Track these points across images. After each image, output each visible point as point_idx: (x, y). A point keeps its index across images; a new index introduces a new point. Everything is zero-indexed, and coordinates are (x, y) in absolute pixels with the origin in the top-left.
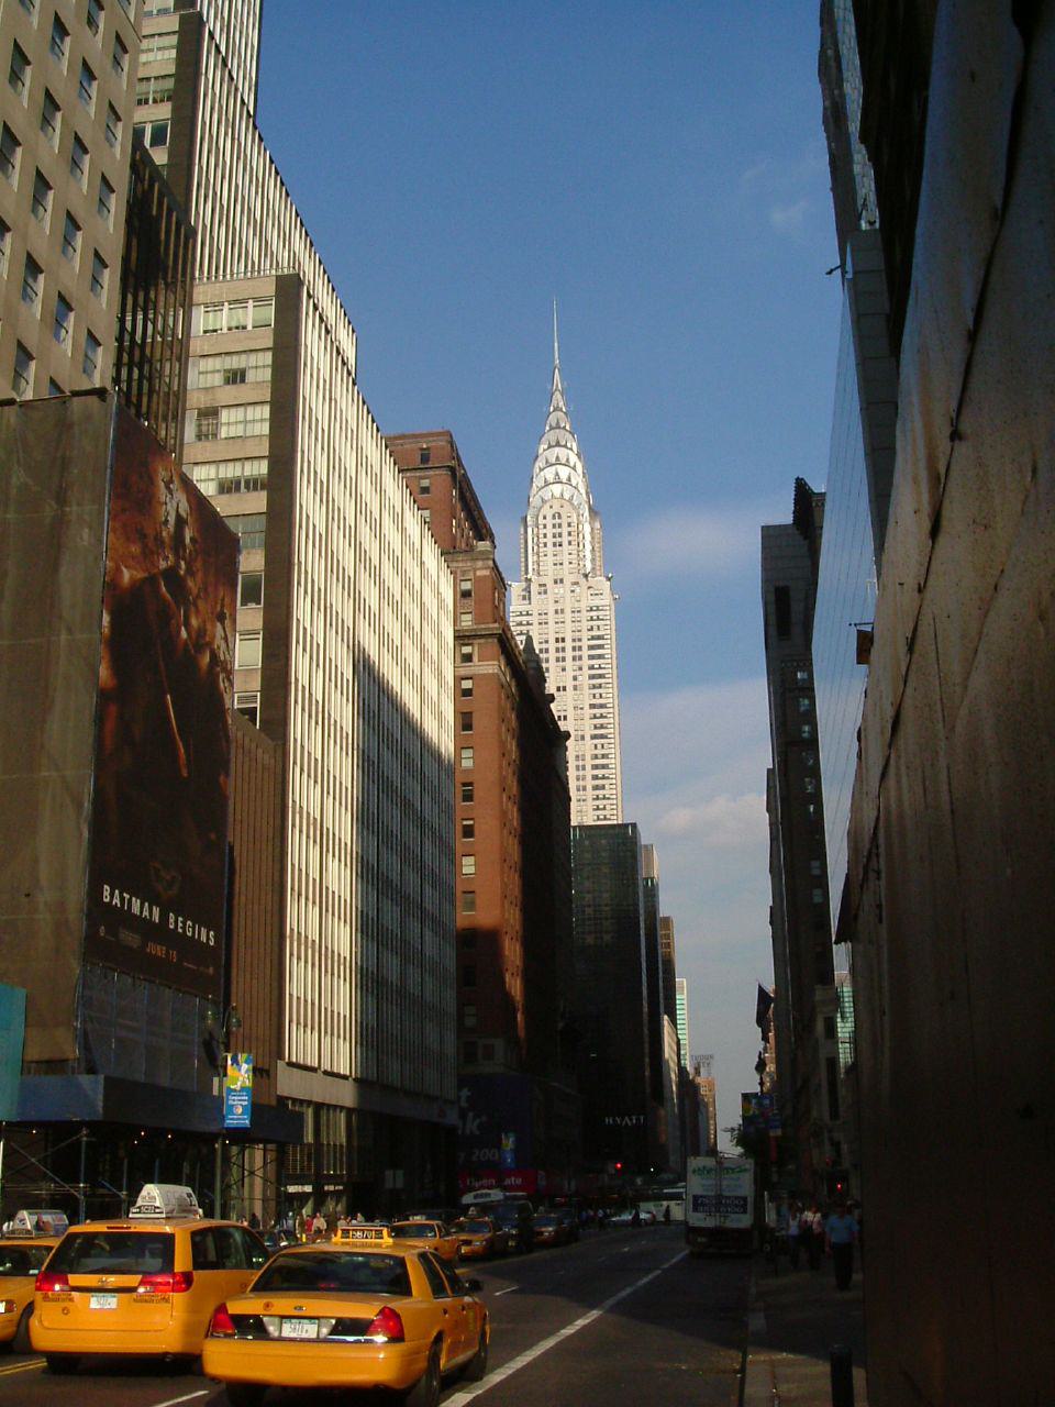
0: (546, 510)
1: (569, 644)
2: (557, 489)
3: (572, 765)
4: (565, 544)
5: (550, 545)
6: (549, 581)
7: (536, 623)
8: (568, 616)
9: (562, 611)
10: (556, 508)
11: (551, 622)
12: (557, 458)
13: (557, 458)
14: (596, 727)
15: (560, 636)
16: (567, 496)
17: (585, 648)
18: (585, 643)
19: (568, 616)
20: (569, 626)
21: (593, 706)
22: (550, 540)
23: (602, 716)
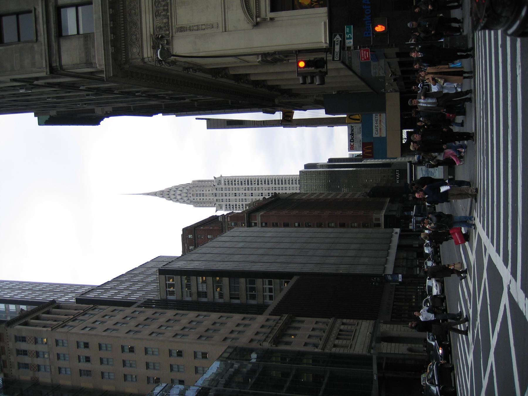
0: (192, 199)
1: (237, 192)
3: (284, 191)
4: (203, 192)
5: (203, 198)
6: (215, 198)
7: (229, 203)
8: (227, 192)
10: (191, 195)
11: (229, 198)
12: (174, 195)
13: (174, 195)
14: (272, 183)
16: (187, 191)
17: (248, 186)
18: (247, 186)
20: (231, 192)
21: (258, 184)
22: (202, 198)
23: (262, 181)
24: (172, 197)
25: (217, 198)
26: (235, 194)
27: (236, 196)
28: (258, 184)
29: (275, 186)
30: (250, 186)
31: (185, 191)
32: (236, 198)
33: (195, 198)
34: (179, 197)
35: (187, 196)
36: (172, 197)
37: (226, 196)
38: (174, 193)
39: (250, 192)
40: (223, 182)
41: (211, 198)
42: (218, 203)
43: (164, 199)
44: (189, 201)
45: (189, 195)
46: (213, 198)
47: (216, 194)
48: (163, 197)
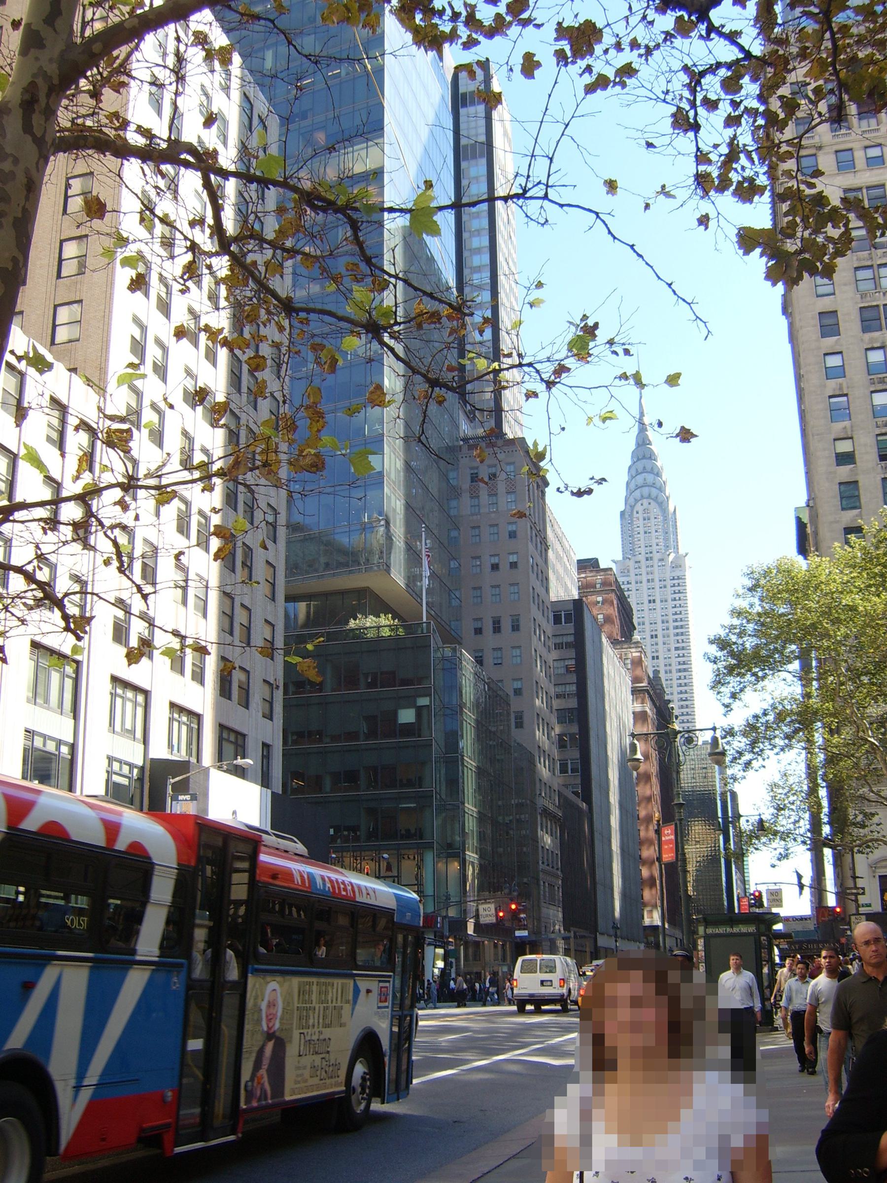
0: (638, 507)
2: (645, 491)
6: (641, 558)
8: (657, 584)
9: (653, 580)
15: (651, 598)
19: (657, 584)
21: (677, 649)
24: (640, 465)
25: (644, 563)
26: (654, 601)
27: (650, 602)
28: (677, 649)
29: (674, 671)
30: (672, 631)
31: (654, 492)
32: (646, 602)
33: (640, 516)
34: (640, 479)
35: (642, 497)
36: (640, 465)
37: (648, 581)
38: (648, 468)
39: (660, 633)
40: (677, 573)
41: (643, 550)
42: (631, 564)
43: (633, 447)
44: (631, 501)
45: (645, 502)
46: (643, 553)
47: (651, 558)
48: (638, 445)
